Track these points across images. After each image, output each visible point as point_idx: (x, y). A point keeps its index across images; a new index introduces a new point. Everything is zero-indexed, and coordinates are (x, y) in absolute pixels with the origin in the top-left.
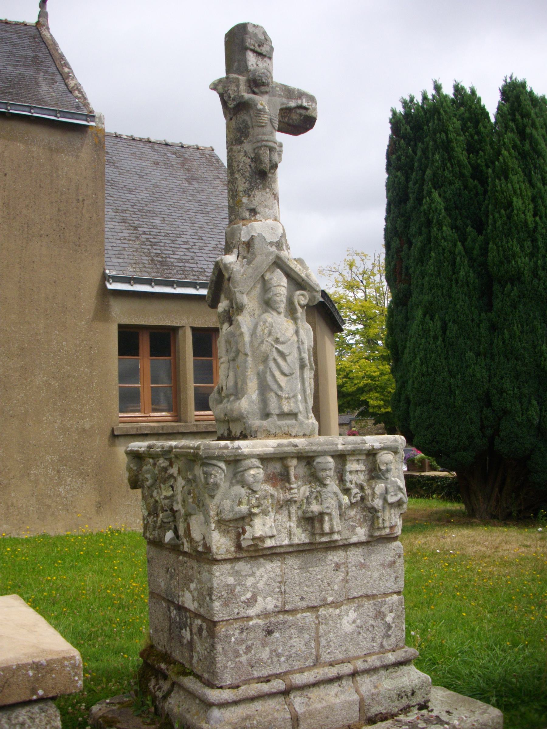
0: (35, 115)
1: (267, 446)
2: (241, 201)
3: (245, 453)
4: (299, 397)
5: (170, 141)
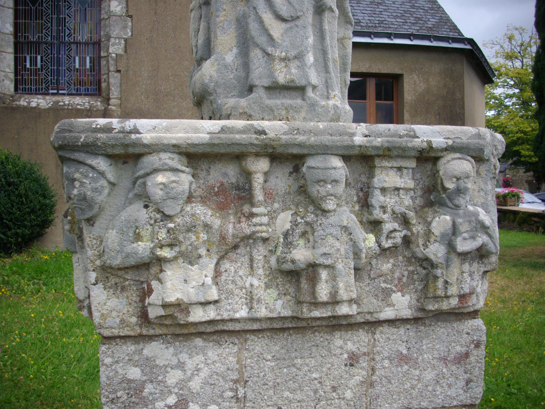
1: (196, 130)
3: (145, 142)
4: (310, 58)
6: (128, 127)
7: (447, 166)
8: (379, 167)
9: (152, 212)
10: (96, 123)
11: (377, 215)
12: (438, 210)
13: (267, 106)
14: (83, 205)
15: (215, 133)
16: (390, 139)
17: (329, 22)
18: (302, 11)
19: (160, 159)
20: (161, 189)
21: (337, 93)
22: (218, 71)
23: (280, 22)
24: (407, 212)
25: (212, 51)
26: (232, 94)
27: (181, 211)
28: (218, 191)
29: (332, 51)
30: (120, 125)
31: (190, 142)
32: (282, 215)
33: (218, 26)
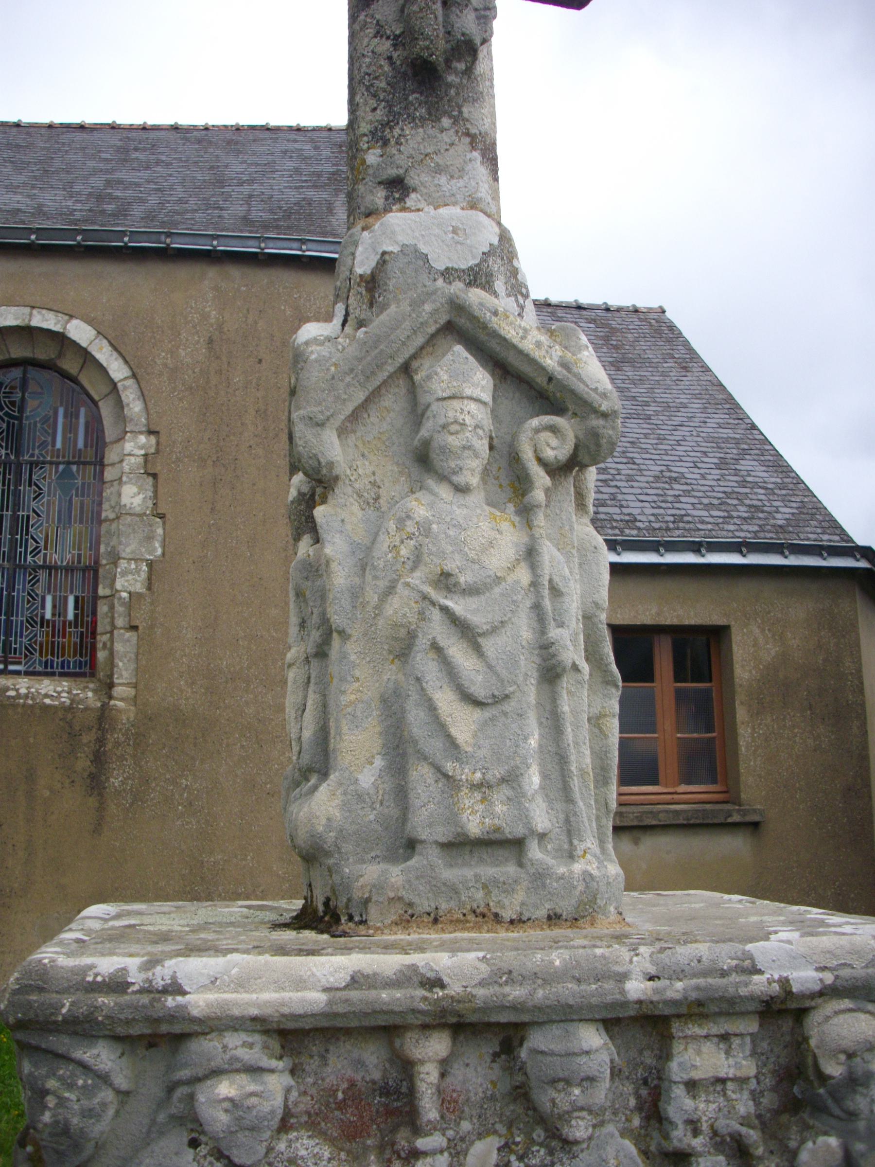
0: (308, 253)
1: (300, 984)
2: (364, 161)
3: (195, 1012)
4: (534, 779)
5: (584, 300)
6: (159, 980)
7: (825, 1027)
8: (679, 1038)
9: (205, 1157)
10: (95, 971)
11: (680, 1140)
12: (811, 1122)
13: (445, 884)
14: (62, 1144)
15: (337, 989)
16: (701, 981)
17: (569, 693)
18: (515, 683)
19: (225, 1047)
20: (226, 1111)
21: (589, 845)
22: (345, 806)
23: (470, 708)
24: (744, 1130)
25: (332, 755)
26: (373, 854)
27: (267, 1153)
28: (344, 1100)
29: (579, 752)
30: (143, 976)
31: (286, 1010)
32: (479, 1147)
33: (344, 712)
